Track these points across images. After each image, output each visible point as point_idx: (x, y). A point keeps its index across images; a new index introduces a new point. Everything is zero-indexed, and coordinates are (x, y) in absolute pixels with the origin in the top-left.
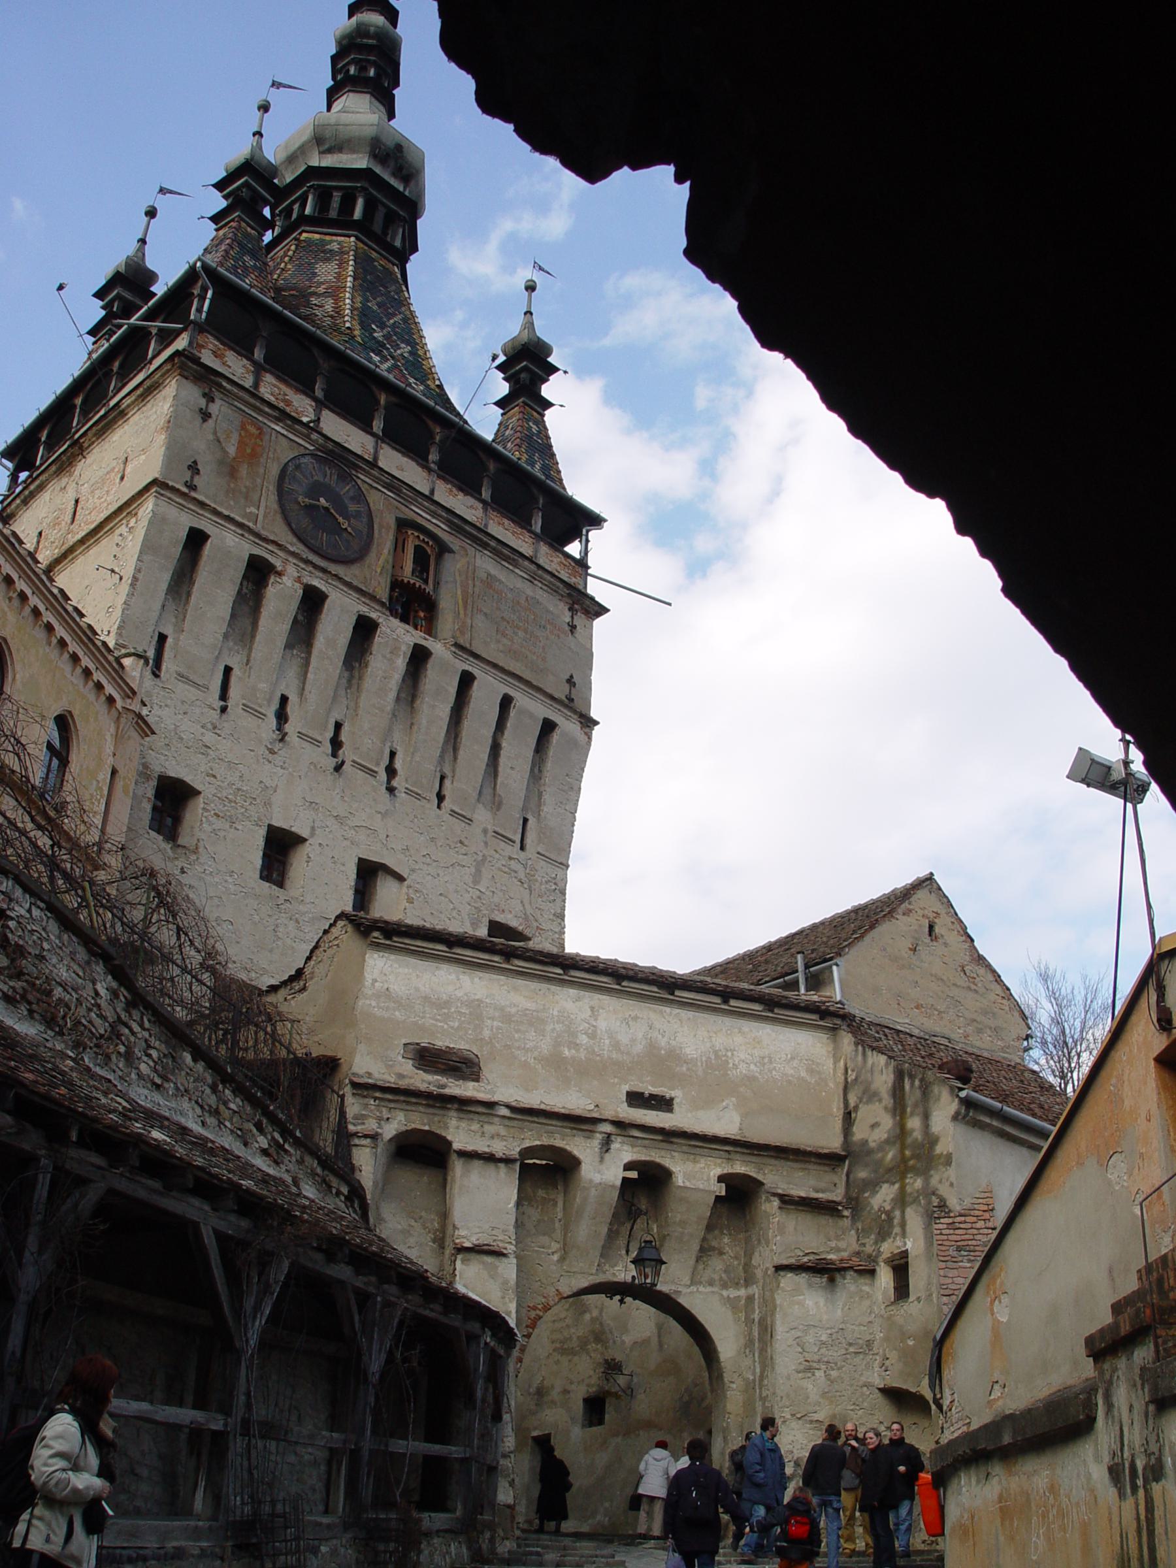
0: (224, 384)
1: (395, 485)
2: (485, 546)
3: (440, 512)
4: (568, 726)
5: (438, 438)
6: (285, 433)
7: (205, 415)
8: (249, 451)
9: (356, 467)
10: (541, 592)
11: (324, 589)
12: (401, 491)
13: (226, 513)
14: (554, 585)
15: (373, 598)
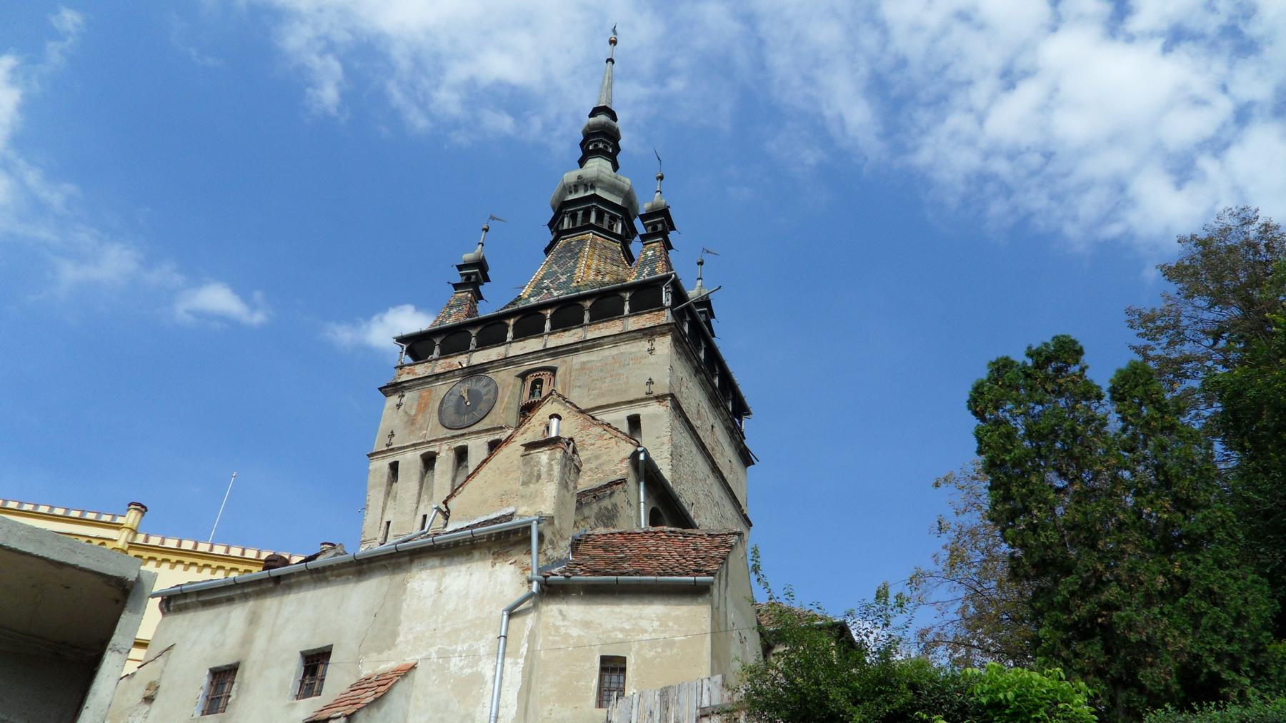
0: (405, 385)
1: (507, 361)
2: (577, 350)
3: (540, 354)
4: (648, 412)
5: (549, 315)
6: (444, 382)
7: (399, 406)
8: (423, 405)
9: (485, 370)
10: (624, 347)
11: (465, 444)
12: (514, 362)
13: (403, 445)
14: (632, 337)
15: (494, 429)
